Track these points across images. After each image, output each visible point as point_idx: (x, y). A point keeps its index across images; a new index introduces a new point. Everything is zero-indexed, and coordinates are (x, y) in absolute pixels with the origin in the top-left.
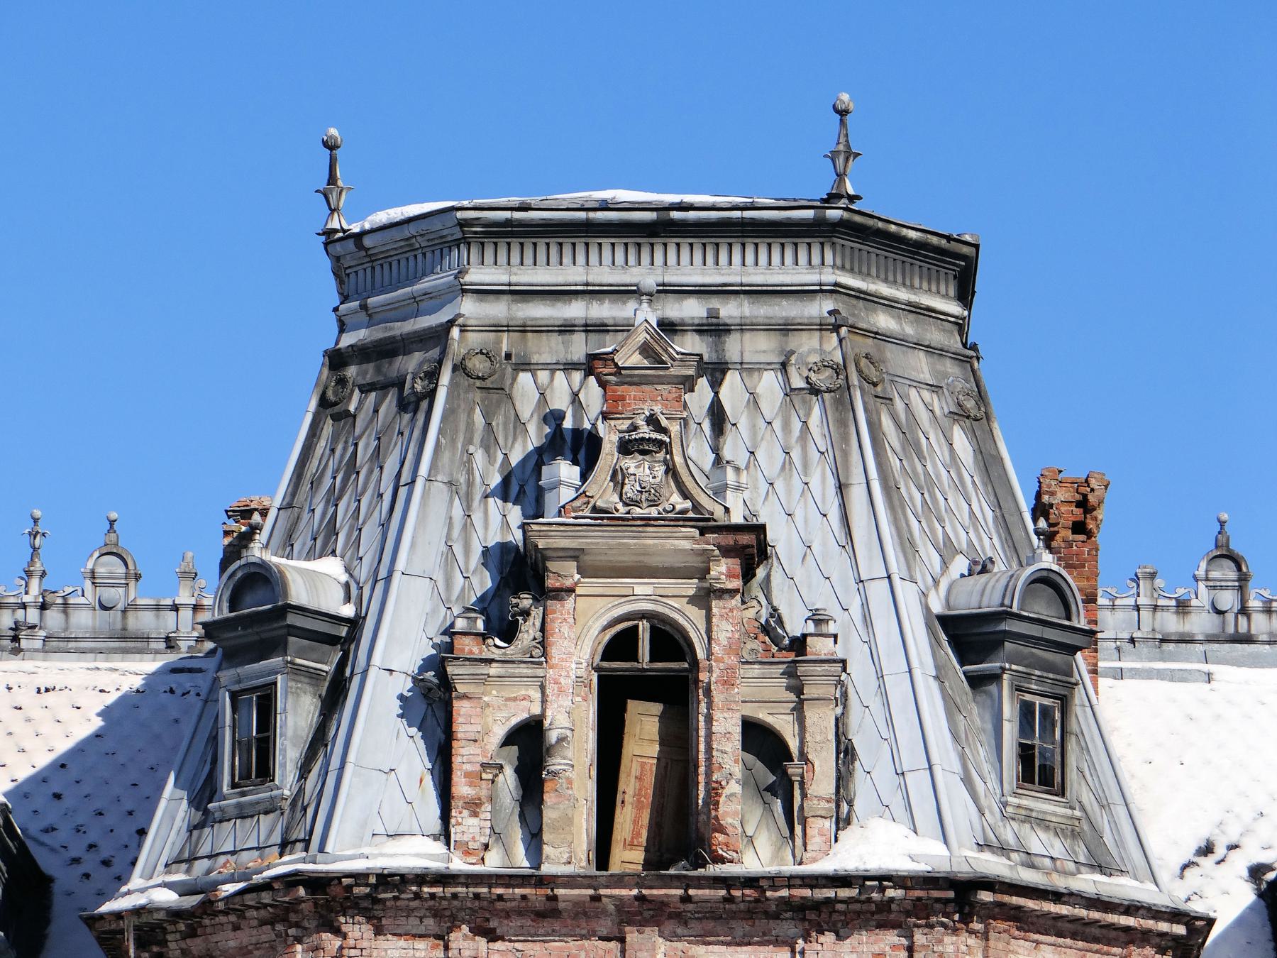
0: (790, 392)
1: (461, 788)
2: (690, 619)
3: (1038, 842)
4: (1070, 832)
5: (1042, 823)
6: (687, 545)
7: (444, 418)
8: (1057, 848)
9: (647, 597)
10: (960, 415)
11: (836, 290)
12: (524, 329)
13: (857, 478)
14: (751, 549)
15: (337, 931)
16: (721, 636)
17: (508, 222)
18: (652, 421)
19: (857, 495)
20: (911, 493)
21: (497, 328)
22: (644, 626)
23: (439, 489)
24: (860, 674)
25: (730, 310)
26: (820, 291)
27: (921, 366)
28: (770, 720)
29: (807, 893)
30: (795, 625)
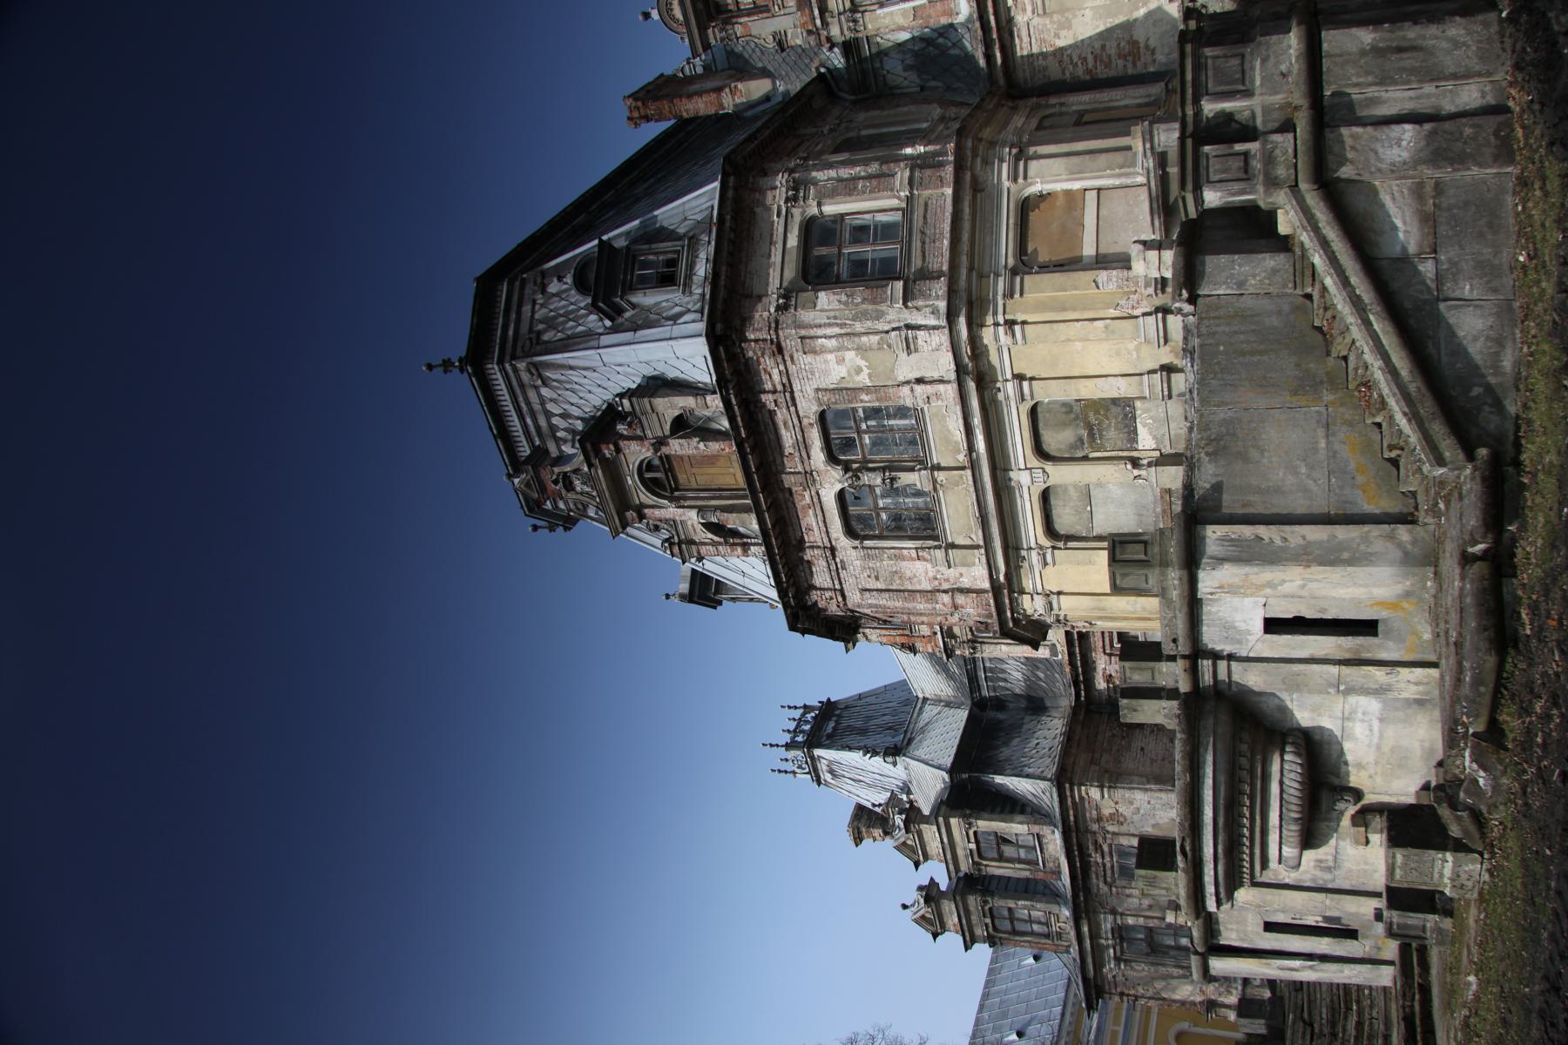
5: (691, 266)
8: (703, 255)
18: (556, 482)
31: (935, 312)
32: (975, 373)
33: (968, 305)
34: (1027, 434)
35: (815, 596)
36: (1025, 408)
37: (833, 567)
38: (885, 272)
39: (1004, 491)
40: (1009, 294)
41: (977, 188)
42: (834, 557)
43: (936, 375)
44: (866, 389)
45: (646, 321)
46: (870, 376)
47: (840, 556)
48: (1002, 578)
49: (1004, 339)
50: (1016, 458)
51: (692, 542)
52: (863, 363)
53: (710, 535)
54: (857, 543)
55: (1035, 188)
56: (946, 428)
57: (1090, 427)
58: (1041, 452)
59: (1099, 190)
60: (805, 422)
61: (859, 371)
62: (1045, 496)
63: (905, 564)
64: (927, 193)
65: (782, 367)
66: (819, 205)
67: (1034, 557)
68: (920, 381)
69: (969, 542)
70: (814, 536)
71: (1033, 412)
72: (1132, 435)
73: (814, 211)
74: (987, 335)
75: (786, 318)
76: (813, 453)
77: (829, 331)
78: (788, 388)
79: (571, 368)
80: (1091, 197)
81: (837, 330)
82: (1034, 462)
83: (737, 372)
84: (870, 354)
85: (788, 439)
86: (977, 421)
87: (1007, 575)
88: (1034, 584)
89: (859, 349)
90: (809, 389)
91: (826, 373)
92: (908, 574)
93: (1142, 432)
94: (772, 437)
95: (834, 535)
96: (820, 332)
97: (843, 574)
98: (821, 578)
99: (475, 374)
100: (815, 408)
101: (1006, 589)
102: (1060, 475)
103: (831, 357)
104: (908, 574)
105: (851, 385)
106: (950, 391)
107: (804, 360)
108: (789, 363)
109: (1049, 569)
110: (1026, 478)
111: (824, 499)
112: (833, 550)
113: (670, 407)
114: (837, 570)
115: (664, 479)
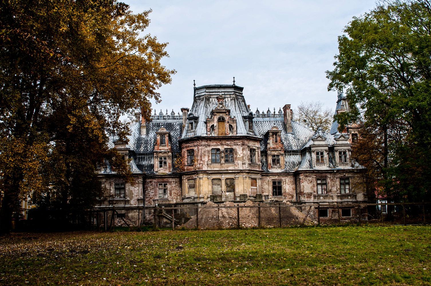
1: (208, 130)
3: (251, 133)
4: (253, 132)
5: (251, 132)
10: (243, 101)
11: (234, 92)
14: (229, 111)
16: (227, 118)
20: (240, 107)
24: (237, 121)
25: (226, 93)
26: (232, 92)
27: (240, 97)
30: (232, 117)
32: (241, 172)
33: (249, 172)
36: (234, 178)
38: (251, 161)
40: (249, 177)
41: (258, 173)
45: (245, 122)
47: (208, 147)
49: (244, 176)
52: (241, 156)
55: (258, 181)
56: (231, 167)
57: (230, 186)
58: (227, 179)
59: (257, 189)
63: (207, 157)
67: (209, 177)
71: (233, 179)
72: (228, 192)
73: (257, 151)
74: (244, 174)
75: (246, 147)
78: (237, 145)
80: (256, 188)
85: (228, 143)
86: (234, 171)
89: (243, 157)
91: (239, 151)
93: (229, 193)
98: (204, 143)
101: (205, 172)
102: (223, 182)
103: (242, 152)
107: (241, 148)
110: (224, 177)
112: (209, 146)
113: (234, 125)
115: (221, 120)
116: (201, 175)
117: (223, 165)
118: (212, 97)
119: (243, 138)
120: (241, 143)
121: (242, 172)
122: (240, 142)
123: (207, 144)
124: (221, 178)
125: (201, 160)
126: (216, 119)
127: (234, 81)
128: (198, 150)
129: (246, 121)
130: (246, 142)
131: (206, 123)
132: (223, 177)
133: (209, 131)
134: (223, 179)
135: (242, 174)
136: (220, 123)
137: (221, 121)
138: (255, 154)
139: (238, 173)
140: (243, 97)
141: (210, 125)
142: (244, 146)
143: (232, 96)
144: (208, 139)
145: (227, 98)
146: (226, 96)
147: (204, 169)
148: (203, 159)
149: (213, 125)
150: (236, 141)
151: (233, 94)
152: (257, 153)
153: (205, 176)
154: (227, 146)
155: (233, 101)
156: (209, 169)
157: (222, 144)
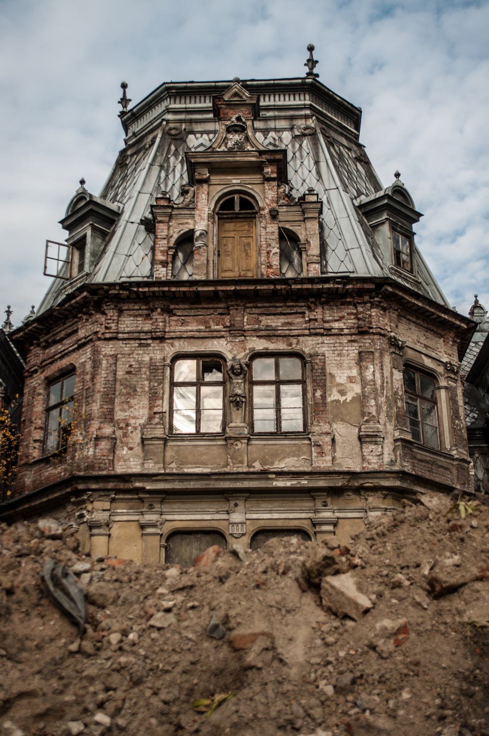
0: (295, 137)
1: (160, 257)
2: (256, 190)
6: (254, 159)
7: (159, 147)
9: (238, 185)
12: (191, 121)
13: (322, 158)
15: (104, 313)
17: (185, 88)
18: (239, 119)
19: (323, 165)
21: (181, 121)
22: (236, 197)
23: (156, 169)
26: (304, 107)
28: (291, 228)
29: (310, 286)
31: (392, 463)
34: (280, 524)
35: (111, 313)
36: (306, 525)
37: (142, 336)
39: (225, 495)
42: (153, 338)
43: (338, 454)
44: (324, 397)
46: (338, 401)
47: (155, 344)
48: (138, 485)
50: (257, 512)
51: (171, 217)
52: (349, 397)
53: (176, 236)
54: (168, 361)
60: (294, 341)
61: (342, 393)
62: (216, 535)
63: (145, 402)
64: (455, 471)
65: (346, 331)
66: (446, 388)
68: (333, 440)
69: (168, 459)
70: (174, 327)
73: (443, 383)
74: (373, 500)
76: (263, 341)
77: (378, 375)
78: (328, 332)
79: (317, 163)
81: (379, 382)
82: (251, 528)
83: (347, 293)
84: (357, 406)
85: (276, 322)
86: (304, 482)
87: (142, 490)
88: (122, 514)
89: (362, 399)
90: (324, 349)
91: (340, 366)
92: (133, 402)
94: (279, 310)
95: (176, 343)
96: (377, 368)
97: (135, 344)
99: (304, 84)
100: (307, 350)
101: (124, 488)
103: (355, 372)
104: (133, 402)
105: (328, 384)
106: (324, 463)
107: (352, 351)
108: (349, 338)
109: (134, 529)
111: (215, 342)
112: (162, 339)
113: (307, 232)
114: (140, 339)
115: (236, 210)
116: (98, 505)
117: (241, 446)
118: (199, 127)
119: (360, 293)
120: (352, 321)
121: (359, 491)
122: (341, 320)
123: (147, 327)
124: (222, 526)
125: (108, 417)
126: (205, 203)
127: (312, 63)
128: (96, 364)
129: (375, 227)
130: (378, 318)
131: (149, 225)
132: (237, 517)
133: (164, 264)
134: (236, 530)
135: (359, 503)
136: (230, 226)
137: (236, 218)
138: (434, 402)
139: (335, 492)
140: (360, 146)
141: (173, 230)
142: (367, 341)
143: (301, 123)
144: (154, 296)
145: (276, 130)
146: (272, 124)
147: (120, 469)
148: (119, 415)
149: (187, 238)
150: (318, 313)
151: (306, 117)
152: (443, 395)
153: (124, 513)
154: (268, 337)
155: (306, 143)
156: (152, 467)
157: (235, 332)
